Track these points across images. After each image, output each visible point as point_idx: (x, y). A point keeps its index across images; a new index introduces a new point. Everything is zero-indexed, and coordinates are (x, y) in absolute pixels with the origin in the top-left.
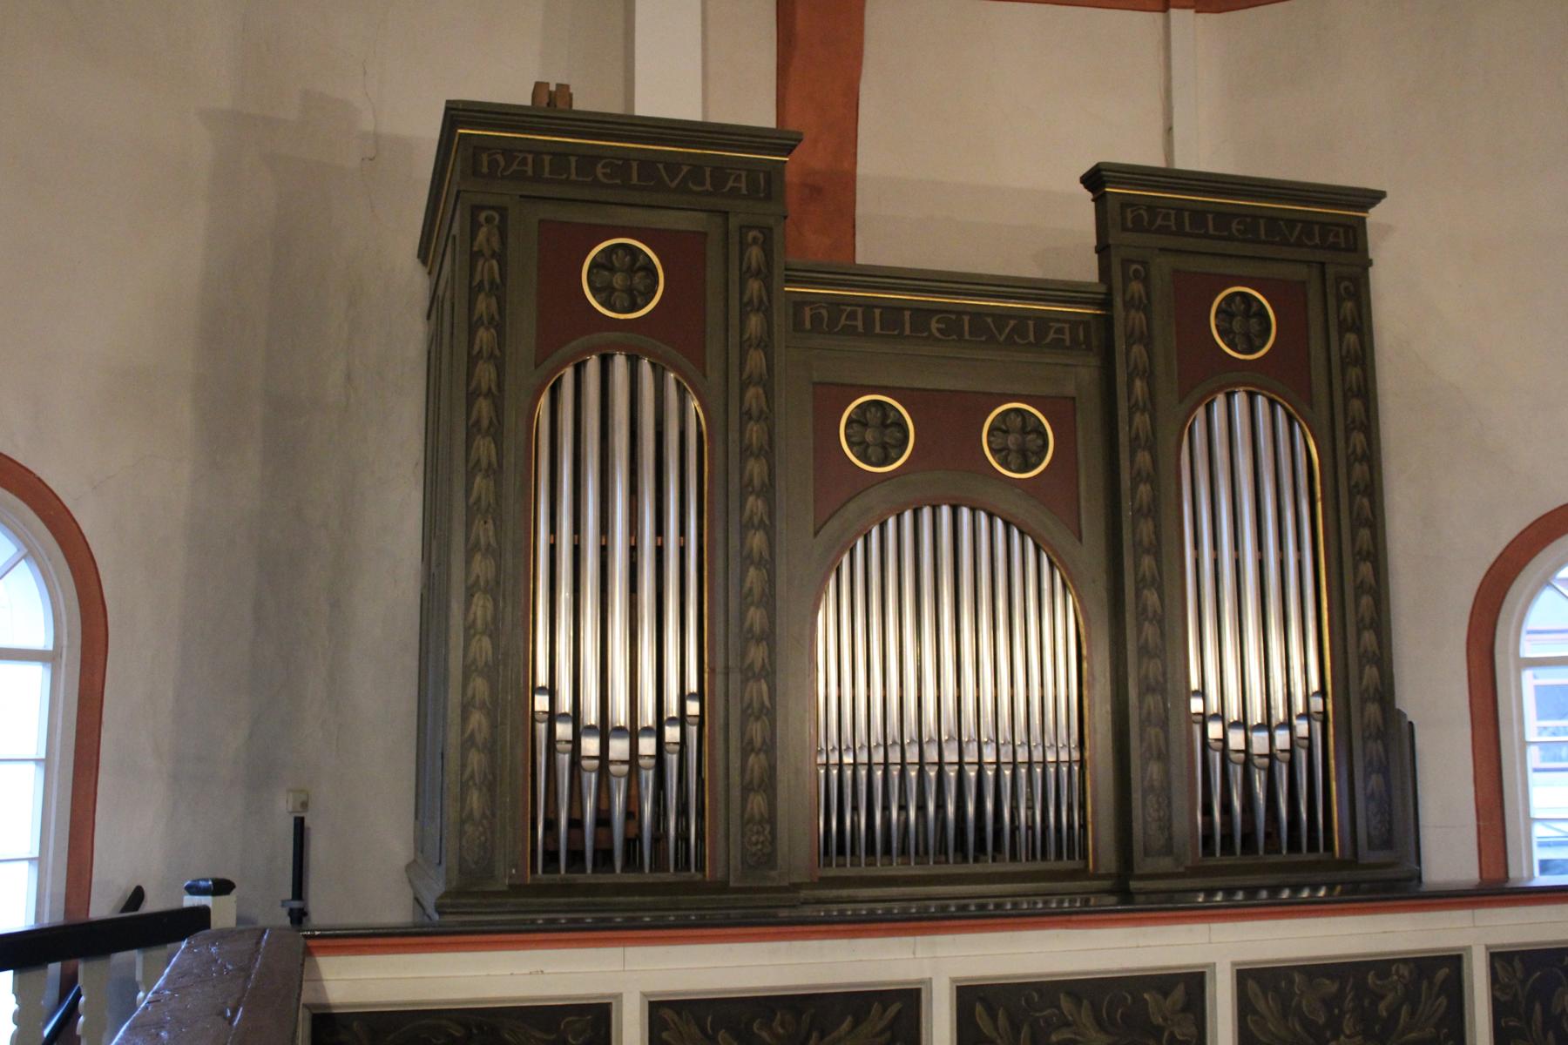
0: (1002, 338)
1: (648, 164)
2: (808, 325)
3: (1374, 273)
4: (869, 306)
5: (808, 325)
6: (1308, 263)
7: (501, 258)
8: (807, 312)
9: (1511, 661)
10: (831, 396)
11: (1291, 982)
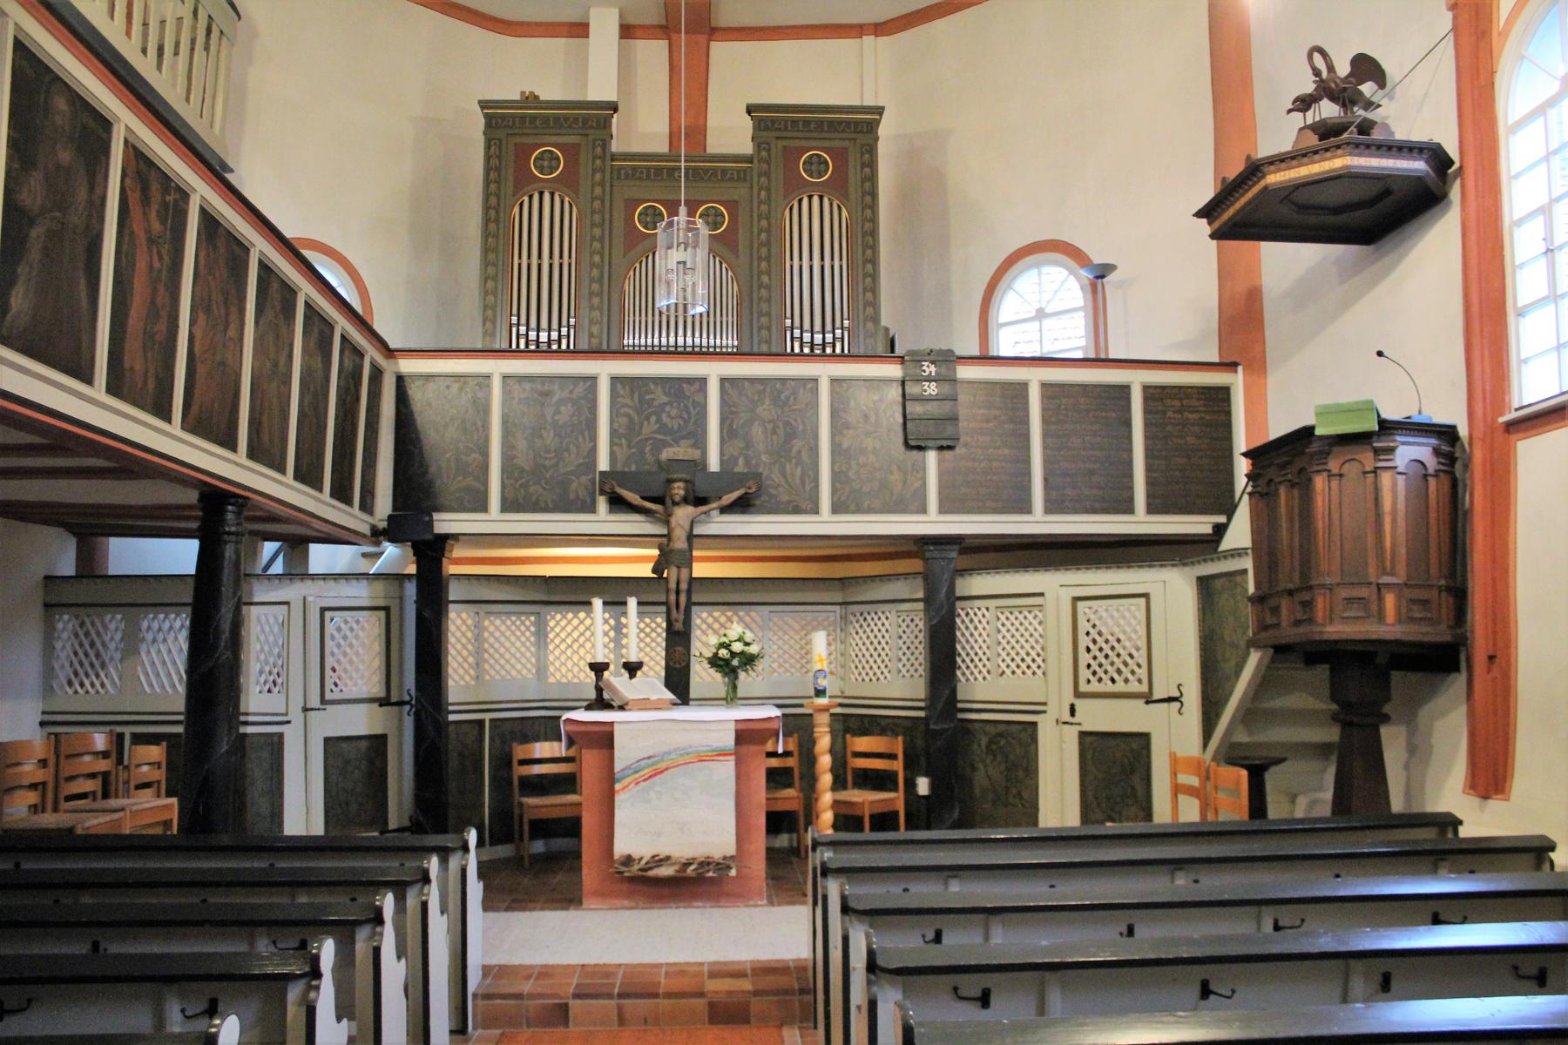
0: (706, 178)
1: (557, 118)
2: (623, 177)
3: (880, 143)
4: (648, 168)
5: (623, 177)
6: (849, 139)
7: (499, 157)
8: (623, 172)
9: (995, 326)
10: (632, 204)
11: (743, 385)
